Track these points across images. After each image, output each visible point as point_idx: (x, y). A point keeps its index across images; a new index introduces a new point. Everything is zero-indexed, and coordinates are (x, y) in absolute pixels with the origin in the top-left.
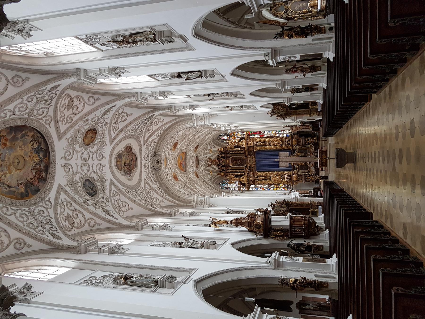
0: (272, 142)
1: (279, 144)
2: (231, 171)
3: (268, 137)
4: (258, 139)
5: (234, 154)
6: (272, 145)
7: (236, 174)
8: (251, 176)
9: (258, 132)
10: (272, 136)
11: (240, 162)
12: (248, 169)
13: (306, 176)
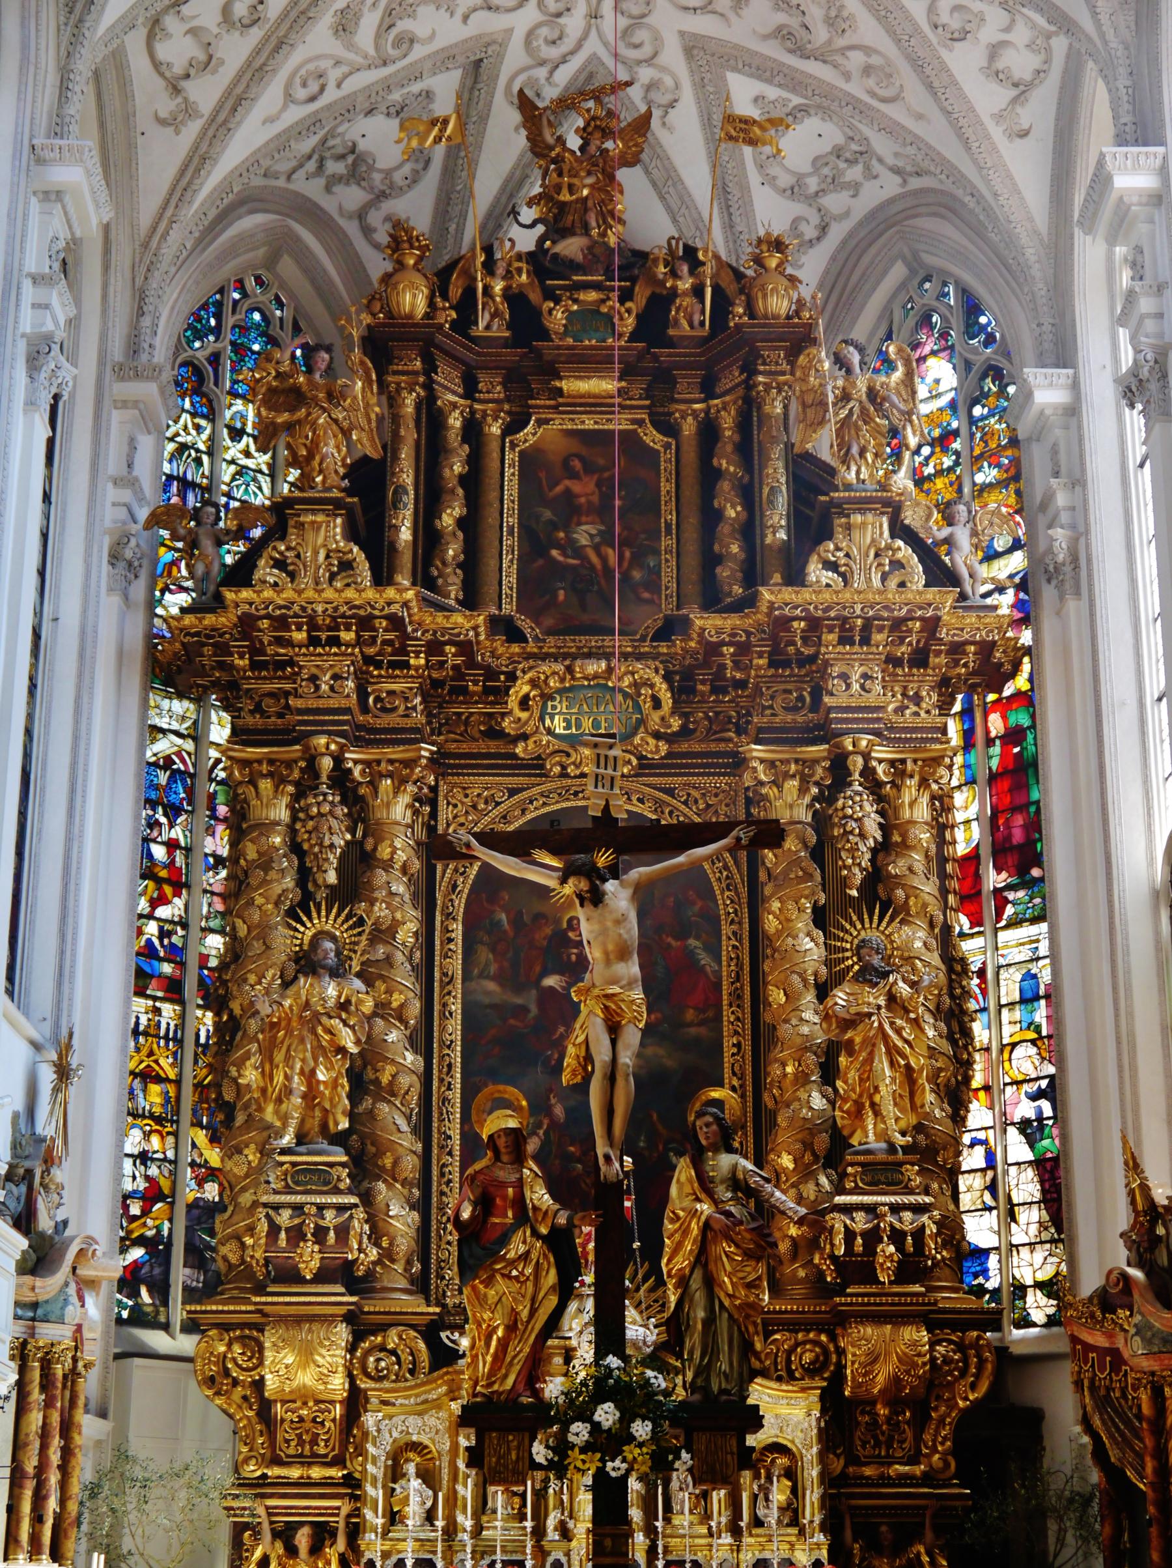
0: (892, 998)
1: (857, 1113)
2: (455, 421)
3: (955, 965)
4: (922, 812)
5: (710, 476)
6: (840, 997)
7: (407, 478)
8: (362, 694)
9: (1035, 826)
10: (967, 1034)
11: (578, 552)
12: (466, 648)
13: (322, 1534)
